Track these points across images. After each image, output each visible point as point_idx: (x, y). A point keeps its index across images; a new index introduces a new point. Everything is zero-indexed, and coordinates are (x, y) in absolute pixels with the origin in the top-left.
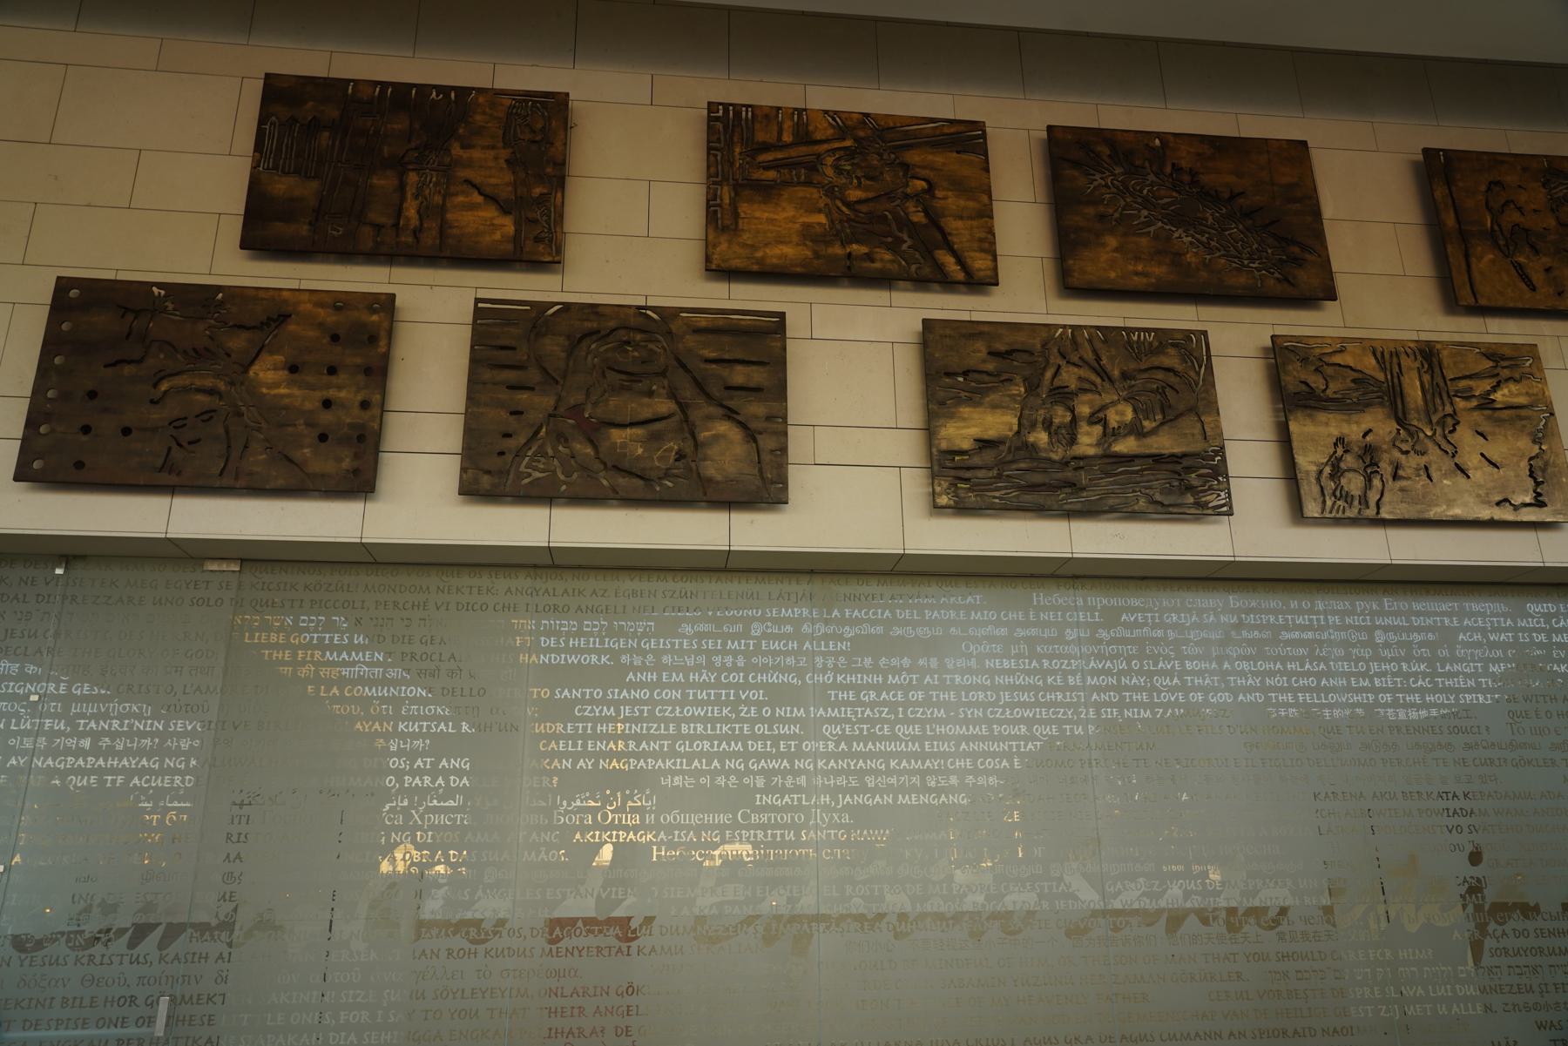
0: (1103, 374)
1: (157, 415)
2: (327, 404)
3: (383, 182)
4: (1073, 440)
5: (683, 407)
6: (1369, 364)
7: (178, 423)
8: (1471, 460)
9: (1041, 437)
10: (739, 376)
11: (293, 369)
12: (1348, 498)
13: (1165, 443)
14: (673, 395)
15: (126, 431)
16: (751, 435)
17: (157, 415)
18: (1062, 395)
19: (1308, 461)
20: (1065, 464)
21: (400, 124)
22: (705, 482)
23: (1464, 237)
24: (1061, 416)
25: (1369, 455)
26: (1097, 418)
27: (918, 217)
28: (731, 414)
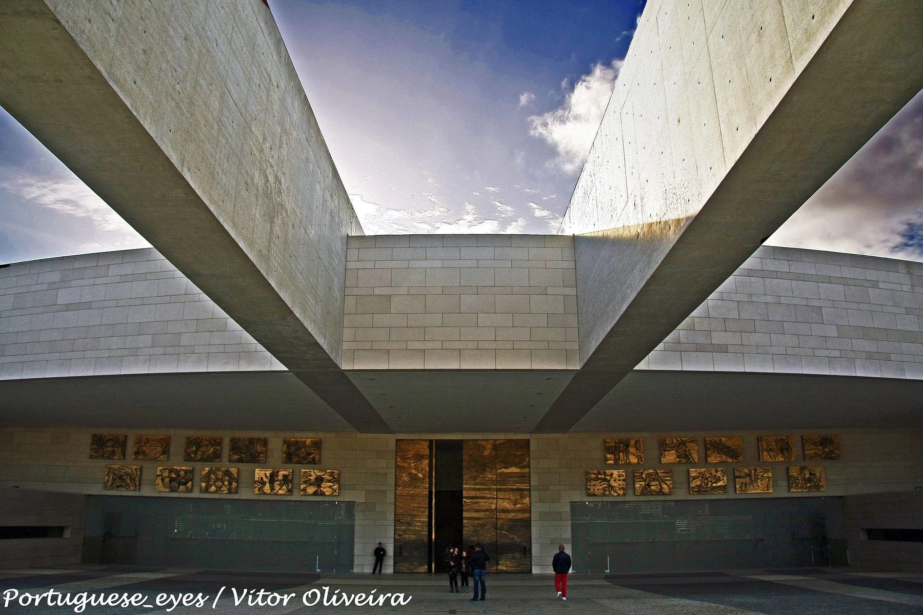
0: (711, 475)
1: (601, 487)
2: (619, 485)
3: (621, 454)
4: (707, 484)
5: (660, 483)
6: (747, 472)
7: (604, 488)
8: (759, 484)
9: (703, 484)
10: (666, 479)
11: (615, 480)
12: (742, 490)
13: (719, 484)
14: (659, 481)
15: (598, 489)
16: (668, 486)
17: (601, 487)
18: (707, 479)
19: (737, 486)
20: (706, 488)
21: (622, 445)
22: (663, 492)
23: (762, 451)
24: (706, 481)
25: (746, 484)
26: (711, 481)
27: (688, 454)
28: (666, 484)
